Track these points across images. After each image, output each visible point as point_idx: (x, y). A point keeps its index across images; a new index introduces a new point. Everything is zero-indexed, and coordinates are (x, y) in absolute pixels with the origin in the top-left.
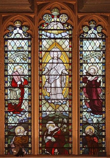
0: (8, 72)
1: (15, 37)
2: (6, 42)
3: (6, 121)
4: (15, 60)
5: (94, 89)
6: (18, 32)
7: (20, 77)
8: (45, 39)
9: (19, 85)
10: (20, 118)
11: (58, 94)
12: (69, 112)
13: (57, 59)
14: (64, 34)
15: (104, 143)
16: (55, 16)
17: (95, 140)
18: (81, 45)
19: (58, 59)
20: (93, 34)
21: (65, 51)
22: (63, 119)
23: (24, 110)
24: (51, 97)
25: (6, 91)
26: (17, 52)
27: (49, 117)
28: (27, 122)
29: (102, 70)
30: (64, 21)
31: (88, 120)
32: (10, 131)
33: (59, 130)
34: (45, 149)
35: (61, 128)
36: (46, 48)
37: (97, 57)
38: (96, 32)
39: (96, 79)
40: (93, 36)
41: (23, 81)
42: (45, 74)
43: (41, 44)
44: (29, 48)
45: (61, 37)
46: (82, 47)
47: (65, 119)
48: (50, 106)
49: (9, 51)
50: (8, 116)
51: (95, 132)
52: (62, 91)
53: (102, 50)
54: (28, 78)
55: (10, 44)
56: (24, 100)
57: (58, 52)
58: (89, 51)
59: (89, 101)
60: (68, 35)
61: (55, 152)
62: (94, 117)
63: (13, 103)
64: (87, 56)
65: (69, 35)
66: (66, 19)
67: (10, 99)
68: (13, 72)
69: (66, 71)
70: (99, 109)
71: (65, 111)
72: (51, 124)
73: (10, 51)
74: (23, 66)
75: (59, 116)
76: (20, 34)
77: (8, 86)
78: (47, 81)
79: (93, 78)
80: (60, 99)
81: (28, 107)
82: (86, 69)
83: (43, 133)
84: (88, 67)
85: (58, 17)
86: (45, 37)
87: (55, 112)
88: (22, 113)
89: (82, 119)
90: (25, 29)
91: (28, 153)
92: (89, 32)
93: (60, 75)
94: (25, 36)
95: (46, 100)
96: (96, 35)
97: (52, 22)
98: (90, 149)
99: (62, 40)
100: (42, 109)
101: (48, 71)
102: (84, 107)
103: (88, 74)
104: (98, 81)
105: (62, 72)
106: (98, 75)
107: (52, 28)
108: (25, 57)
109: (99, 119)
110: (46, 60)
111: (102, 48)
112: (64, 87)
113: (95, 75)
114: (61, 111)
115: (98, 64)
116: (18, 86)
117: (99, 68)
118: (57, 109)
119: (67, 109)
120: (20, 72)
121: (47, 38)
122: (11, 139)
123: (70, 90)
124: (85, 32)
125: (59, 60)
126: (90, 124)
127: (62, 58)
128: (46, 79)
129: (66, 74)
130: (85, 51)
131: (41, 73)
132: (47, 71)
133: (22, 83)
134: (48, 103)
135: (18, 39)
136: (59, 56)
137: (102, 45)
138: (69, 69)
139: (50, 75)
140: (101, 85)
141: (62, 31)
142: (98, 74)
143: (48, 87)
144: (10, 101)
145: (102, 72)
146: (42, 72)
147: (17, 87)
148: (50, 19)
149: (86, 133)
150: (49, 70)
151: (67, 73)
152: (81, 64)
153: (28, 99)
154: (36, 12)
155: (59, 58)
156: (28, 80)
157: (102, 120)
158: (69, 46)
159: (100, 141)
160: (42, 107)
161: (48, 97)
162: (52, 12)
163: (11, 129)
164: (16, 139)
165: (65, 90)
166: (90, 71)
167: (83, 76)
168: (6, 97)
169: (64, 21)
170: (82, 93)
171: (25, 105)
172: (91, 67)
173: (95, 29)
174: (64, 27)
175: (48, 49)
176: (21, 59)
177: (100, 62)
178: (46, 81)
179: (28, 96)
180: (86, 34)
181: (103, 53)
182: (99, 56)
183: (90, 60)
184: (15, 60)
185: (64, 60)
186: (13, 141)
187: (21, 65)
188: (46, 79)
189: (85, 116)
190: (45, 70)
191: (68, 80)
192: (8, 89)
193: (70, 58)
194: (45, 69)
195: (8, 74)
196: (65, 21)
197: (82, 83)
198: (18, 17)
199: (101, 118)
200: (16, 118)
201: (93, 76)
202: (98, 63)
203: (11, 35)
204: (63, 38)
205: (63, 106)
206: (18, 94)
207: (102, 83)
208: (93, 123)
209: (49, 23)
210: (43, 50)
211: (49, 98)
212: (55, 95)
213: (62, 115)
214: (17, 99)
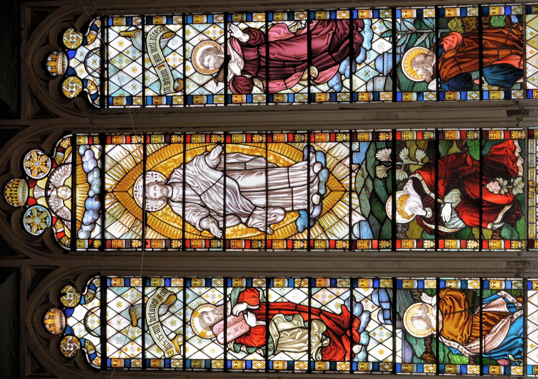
0: (214, 359)
1: (98, 331)
2: (114, 363)
3: (387, 367)
4: (172, 332)
5: (271, 50)
6: (79, 322)
7: (232, 317)
8: (103, 230)
9: (258, 320)
10: (376, 319)
11: (289, 183)
12: (351, 141)
13: (169, 185)
14: (89, 165)
15: (464, 10)
16: (31, 195)
17: (453, 42)
18: (125, 103)
19: (171, 181)
20: (90, 61)
21: (145, 157)
22: (381, 163)
23: (346, 304)
24: (301, 207)
25: (280, 366)
26: (148, 326)
27: (371, 212)
28: (391, 293)
29: (209, 25)
30: (46, 162)
31: (383, 73)
32: (421, 358)
33: (417, 175)
34: (486, 228)
35: (413, 168)
36: (133, 226)
37: (163, 45)
38: (83, 51)
39: (237, 45)
40: (94, 62)
41: (242, 307)
42: (220, 229)
43: (120, 242)
44: (132, 285)
45: (96, 174)
46: (130, 99)
47: (378, 156)
48: (330, 211)
49: (143, 353)
50: (366, 360)
51: (426, 47)
52: (278, 167)
53: (140, 27)
54: (234, 288)
55: (119, 349)
56: (310, 302)
57: (147, 182)
58: (143, 73)
59: (314, 70)
60: (90, 149)
61: (500, 191)
62: (371, 49)
63: (322, 341)
64: (159, 80)
65: (92, 146)
66: (38, 155)
67: (309, 351)
68: (214, 339)
69: (210, 152)
70: (341, 31)
71: (351, 156)
72: (398, 206)
73: (144, 350)
74: (193, 305)
75: (369, 175)
76: (86, 316)
77: (261, 358)
78: (244, 220)
79: (234, 55)
80: (306, 175)
81: (334, 290)
82: (204, 84)
83: (429, 236)
84: (197, 78)
85: (31, 183)
86: (98, 229)
87: (353, 191)
88: (357, 311)
89: (379, 92)
90: (70, 296)
91: (499, 291)
92: (82, 77)
93: (225, 176)
94: (95, 297)
95: (311, 224)
96: (90, 51)
97: (48, 203)
98: (485, 60)
99: (107, 167)
100: (342, 240)
101: (211, 217)
102: (337, 88)
103: (222, 75)
104: (245, 38)
105: (215, 168)
106: (226, 39)
107: (69, 203)
108: (165, 298)
109: (378, 31)
110: (175, 225)
111: (135, 26)
112: (267, 162)
113: (226, 47)
114: (351, 171)
115: (188, 42)
116: (264, 323)
117: (202, 37)
118: (342, 184)
119: (342, 150)
120: (212, 316)
121: (99, 222)
122: (450, 351)
123: (275, 138)
124: (83, 88)
125: (175, 181)
126: (396, 66)
127: (165, 169)
128: (238, 225)
129: (221, 154)
130: (144, 87)
131: (219, 244)
132: (211, 220)
133: (251, 311)
134: (320, 216)
135: (104, 322)
136: (159, 179)
137: (123, 28)
138: (205, 142)
139: (225, 211)
140: (258, 25)
141: (79, 169)
142: (222, 40)
143: (267, 218)
144: (313, 352)
145: (213, 23)
146: (215, 238)
147: (267, 327)
148: (38, 211)
149: (428, 78)
150: (209, 216)
151: (219, 149)
152: (187, 99)
153: (306, 290)
154: (15, 263)
155: (168, 179)
156: (242, 287)
157: (383, 20)
158: (126, 143)
159: (455, 24)
160: (334, 238)
161: (300, 216)
162: (18, 204)
163: (414, 354)
164: (451, 334)
165: (278, 155)
166: (210, 69)
167: (229, 92)
168: (301, 365)
169: (46, 162)
170: (288, 94)
171: (327, 300)
172: (198, 63)
173: (69, 53)
174: (64, 164)
175: (136, 218)
176: (168, 314)
177: (180, 33)
178: (247, 226)
179: (298, 288)
180: (89, 85)
181: (152, 24)
182: (162, 37)
183: (174, 69)
184: (172, 332)
185: (175, 161)
186: (457, 344)
187: (189, 312)
188: (238, 225)
189: (366, 83)
190: (209, 230)
191: (241, 146)
192: (273, 361)
193: (168, 142)
194: (204, 230)
195: (222, 357)
196: (45, 158)
197: (252, 95)
198: (32, 322)
199: (372, 24)
200: (374, 334)
201: (227, 58)
202: (185, 42)
203: (90, 347)
204: (99, 166)
205: (331, 162)
206: (289, 326)
207: (252, 25)
208: (391, 51)
209: (53, 215)
210: (141, 233)
211: (304, 214)
212: (292, 192)
213: (363, 166)
214: (305, 328)
